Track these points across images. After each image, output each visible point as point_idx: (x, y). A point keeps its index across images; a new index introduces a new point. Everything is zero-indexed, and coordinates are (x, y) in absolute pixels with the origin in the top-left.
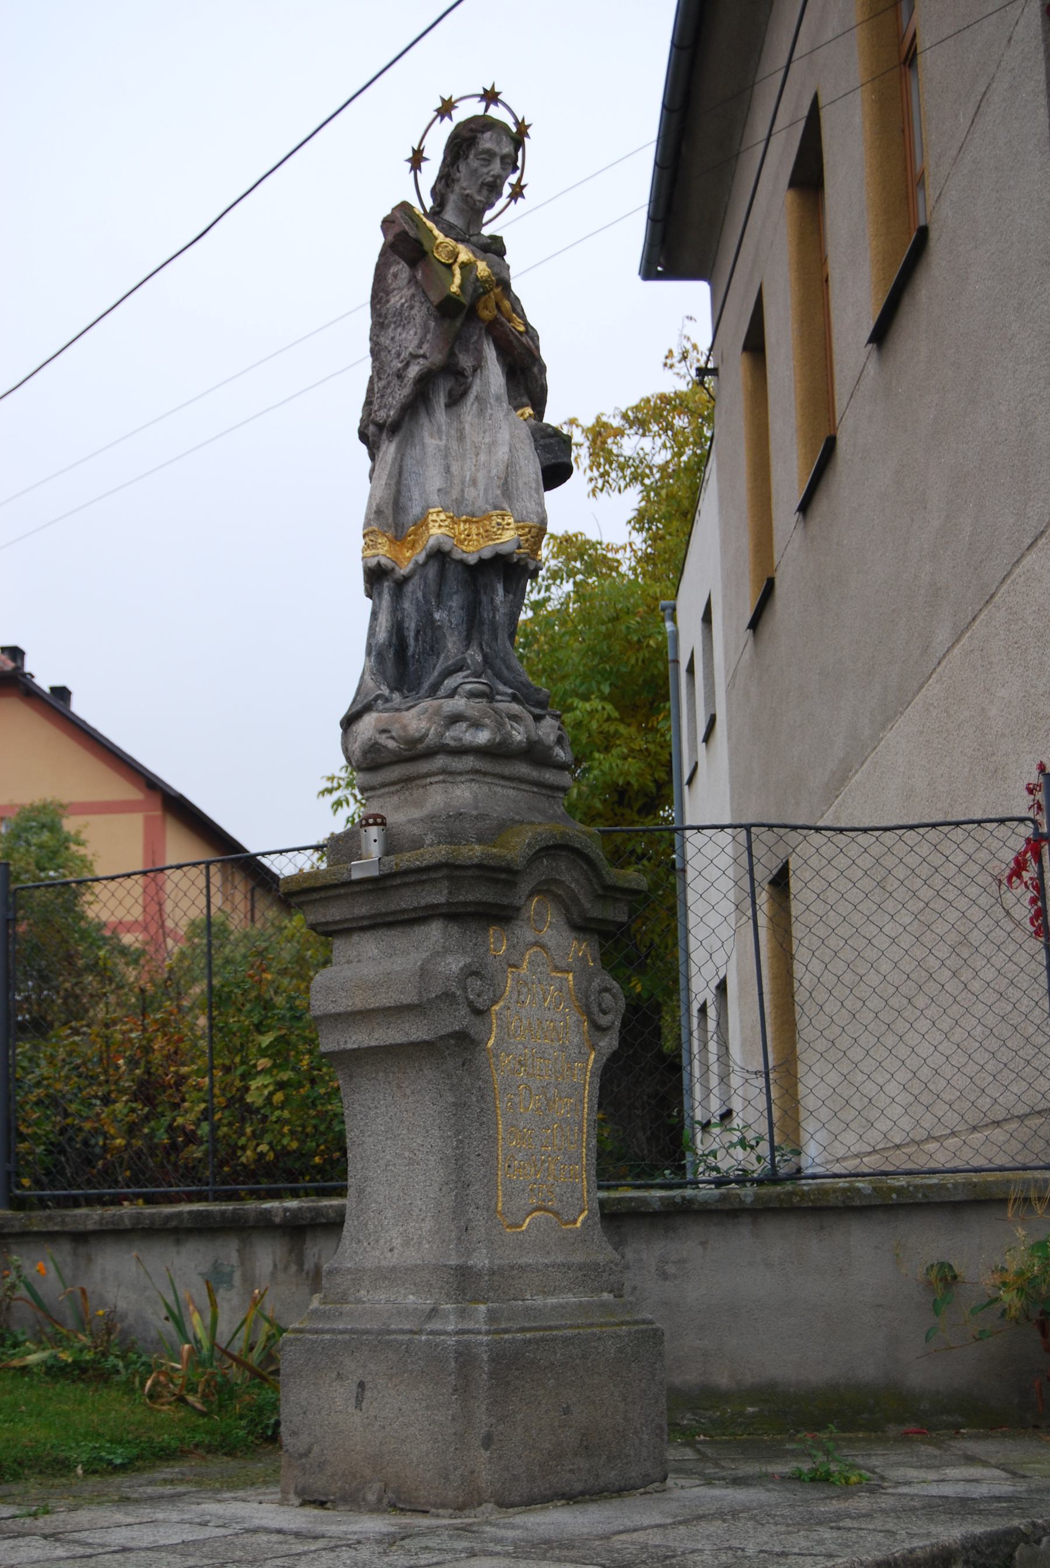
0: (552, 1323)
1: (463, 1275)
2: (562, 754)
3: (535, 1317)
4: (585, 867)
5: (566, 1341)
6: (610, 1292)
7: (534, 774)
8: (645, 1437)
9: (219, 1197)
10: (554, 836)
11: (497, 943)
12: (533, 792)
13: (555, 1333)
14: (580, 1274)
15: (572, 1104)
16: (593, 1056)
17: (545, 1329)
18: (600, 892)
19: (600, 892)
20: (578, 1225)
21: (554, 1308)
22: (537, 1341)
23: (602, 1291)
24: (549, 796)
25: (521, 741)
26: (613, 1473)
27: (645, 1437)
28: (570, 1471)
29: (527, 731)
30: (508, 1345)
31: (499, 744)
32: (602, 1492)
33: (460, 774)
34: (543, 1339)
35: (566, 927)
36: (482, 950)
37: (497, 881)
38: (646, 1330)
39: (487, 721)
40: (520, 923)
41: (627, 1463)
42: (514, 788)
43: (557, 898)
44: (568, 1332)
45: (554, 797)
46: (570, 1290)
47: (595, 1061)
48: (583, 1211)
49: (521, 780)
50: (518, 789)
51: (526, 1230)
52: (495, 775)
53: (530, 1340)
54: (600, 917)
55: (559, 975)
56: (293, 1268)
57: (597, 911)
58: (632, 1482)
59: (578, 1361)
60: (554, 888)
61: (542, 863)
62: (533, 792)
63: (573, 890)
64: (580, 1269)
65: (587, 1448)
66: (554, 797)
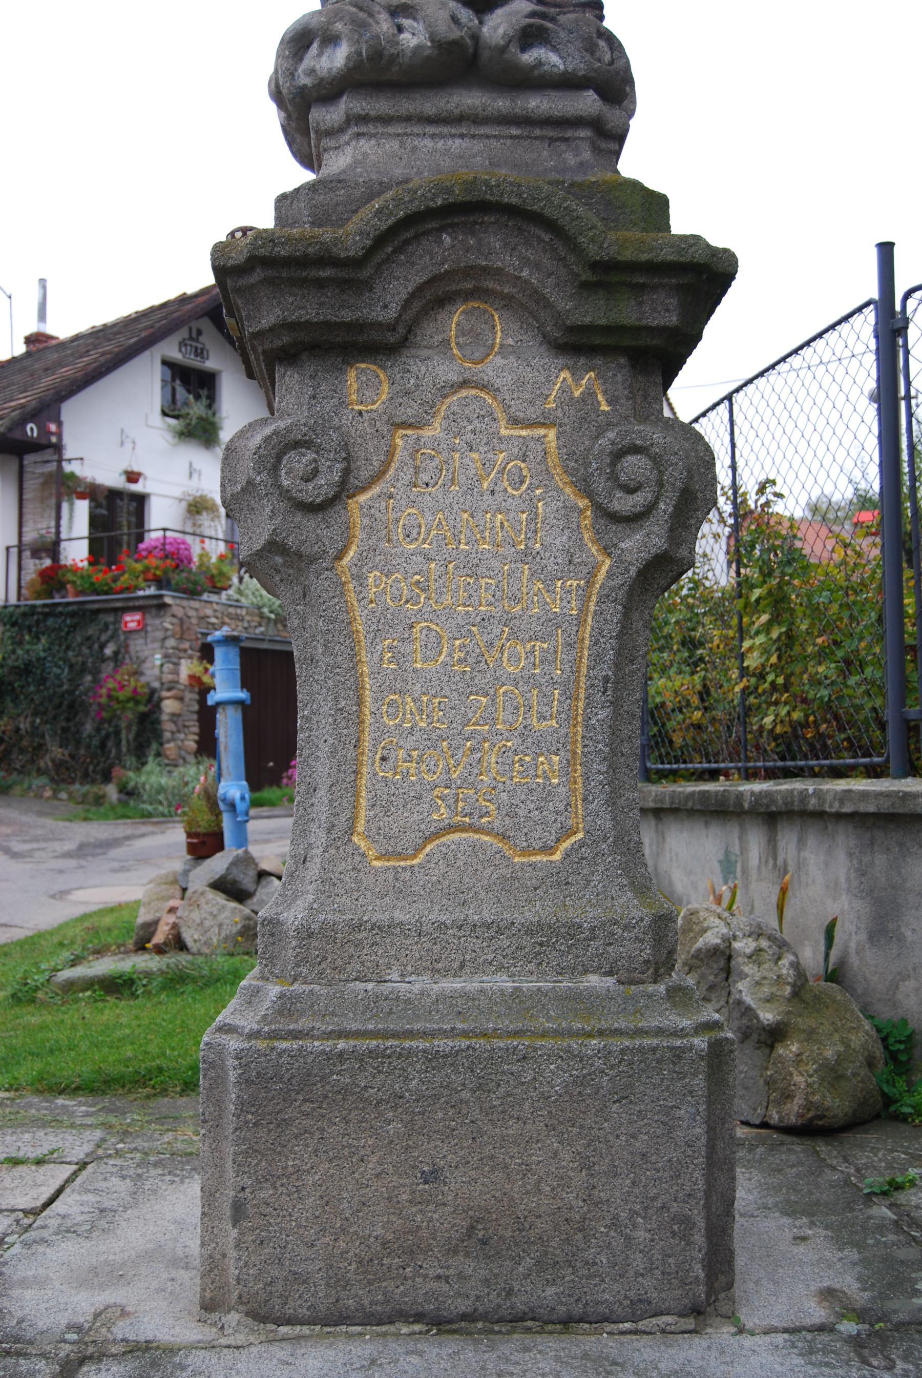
0: (417, 1026)
1: (272, 935)
2: (554, 58)
3: (391, 1012)
4: (547, 237)
5: (433, 1058)
6: (609, 973)
7: (501, 104)
8: (641, 1235)
9: (771, 774)
10: (449, 191)
11: (366, 391)
12: (512, 137)
13: (407, 1044)
14: (527, 941)
15: (542, 650)
16: (605, 568)
17: (395, 1035)
18: (587, 276)
19: (587, 276)
20: (557, 857)
21: (441, 998)
22: (360, 1058)
23: (586, 971)
24: (552, 140)
25: (418, 47)
26: (551, 1291)
27: (641, 1235)
28: (439, 1277)
29: (428, 26)
30: (285, 1059)
31: (371, 59)
32: (522, 1319)
33: (341, 130)
34: (372, 1053)
35: (543, 349)
36: (329, 405)
37: (321, 284)
38: (654, 1050)
39: (339, 26)
40: (425, 353)
41: (590, 1277)
42: (462, 136)
43: (508, 303)
44: (443, 1044)
45: (566, 140)
46: (501, 968)
47: (610, 575)
48: (569, 832)
49: (459, 119)
50: (473, 137)
51: (421, 866)
52: (408, 119)
53: (341, 1054)
54: (603, 322)
55: (524, 433)
56: (771, 862)
57: (593, 312)
58: (601, 1309)
59: (466, 1095)
60: (490, 284)
61: (440, 242)
62: (512, 137)
63: (527, 282)
64: (529, 932)
65: (484, 1242)
66: (566, 140)
